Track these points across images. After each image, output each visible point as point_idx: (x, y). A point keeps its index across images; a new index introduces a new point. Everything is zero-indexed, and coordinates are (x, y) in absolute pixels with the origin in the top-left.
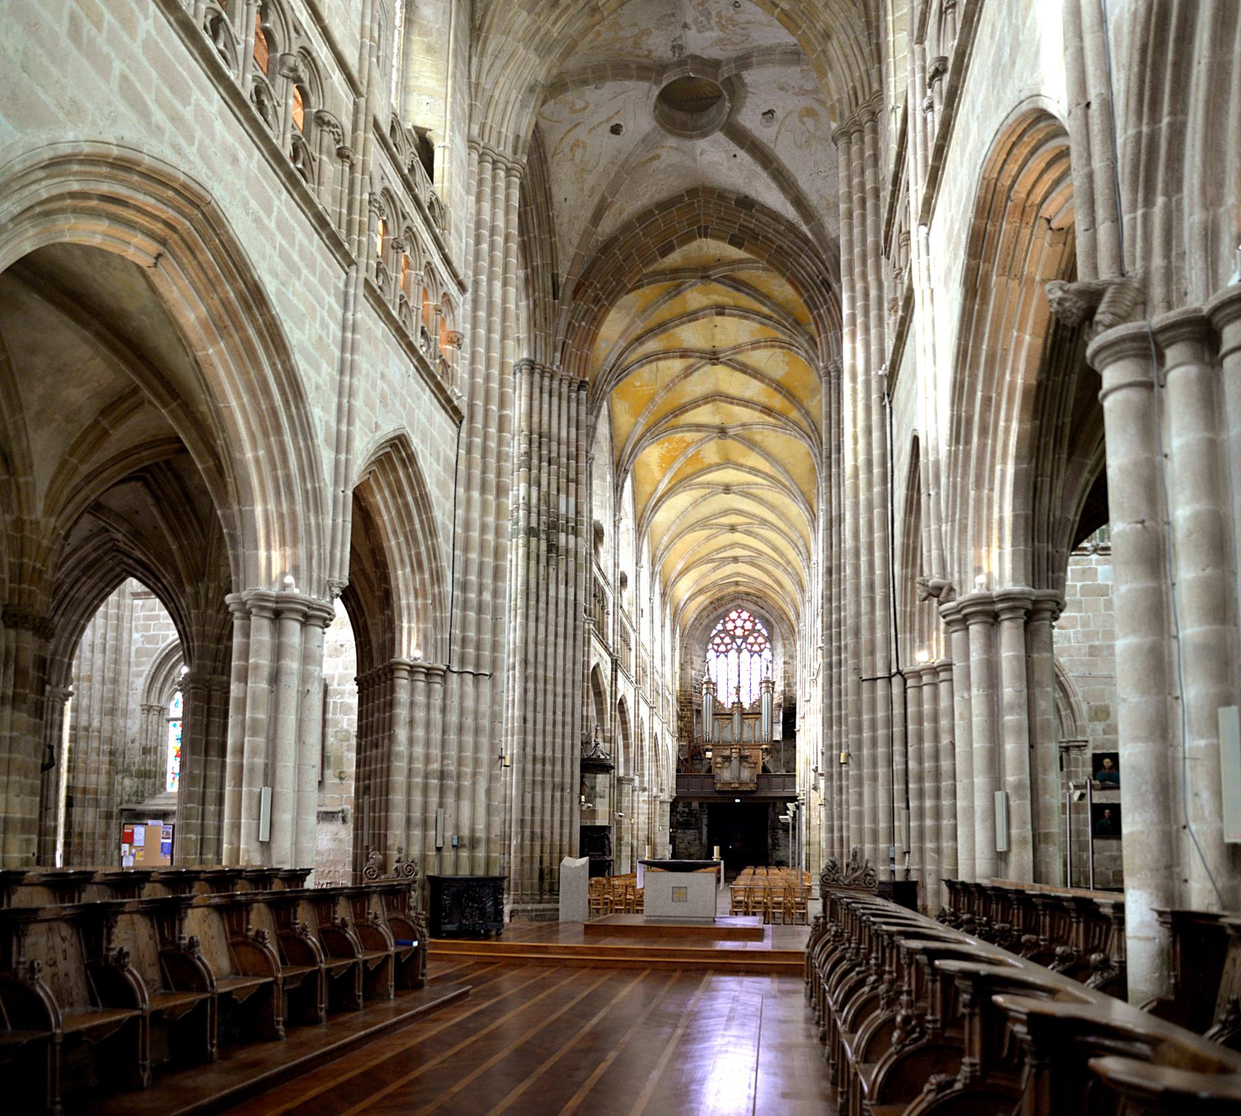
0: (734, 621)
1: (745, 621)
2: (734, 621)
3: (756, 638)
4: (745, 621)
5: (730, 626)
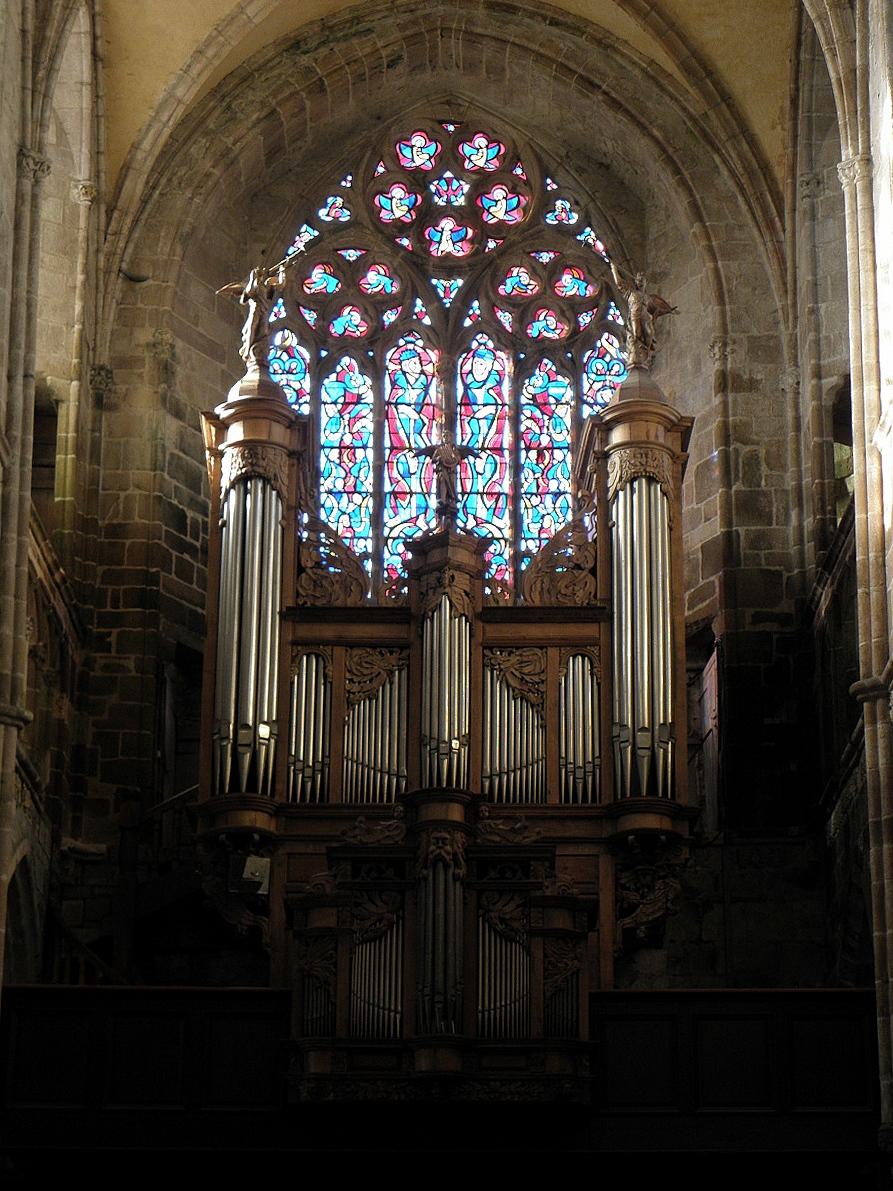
0: (417, 181)
1: (482, 182)
2: (417, 181)
3: (549, 276)
4: (482, 182)
5: (397, 205)
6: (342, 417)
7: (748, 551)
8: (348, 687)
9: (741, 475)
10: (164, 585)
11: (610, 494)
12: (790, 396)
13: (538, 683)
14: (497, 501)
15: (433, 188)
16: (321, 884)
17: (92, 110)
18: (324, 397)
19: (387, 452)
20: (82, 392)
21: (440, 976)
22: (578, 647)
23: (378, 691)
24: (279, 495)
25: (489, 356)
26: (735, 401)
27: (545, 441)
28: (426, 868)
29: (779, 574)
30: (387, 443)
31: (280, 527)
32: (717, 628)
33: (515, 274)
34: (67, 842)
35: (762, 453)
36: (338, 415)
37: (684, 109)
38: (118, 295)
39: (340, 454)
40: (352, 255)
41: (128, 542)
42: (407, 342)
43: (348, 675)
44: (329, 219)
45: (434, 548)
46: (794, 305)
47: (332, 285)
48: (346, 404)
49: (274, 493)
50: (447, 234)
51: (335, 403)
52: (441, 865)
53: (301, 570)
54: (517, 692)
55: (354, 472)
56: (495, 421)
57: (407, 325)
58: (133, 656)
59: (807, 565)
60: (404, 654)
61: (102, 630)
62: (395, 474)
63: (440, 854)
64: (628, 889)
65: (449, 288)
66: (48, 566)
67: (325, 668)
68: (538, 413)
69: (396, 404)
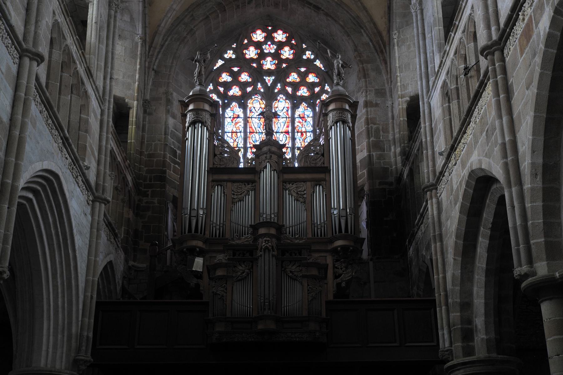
1: (281, 45)
2: (258, 45)
3: (303, 76)
4: (281, 45)
5: (251, 53)
6: (232, 122)
7: (377, 161)
8: (233, 196)
9: (373, 135)
10: (168, 175)
11: (329, 127)
12: (390, 109)
13: (304, 195)
14: (287, 150)
15: (264, 47)
16: (221, 259)
17: (143, 10)
18: (226, 116)
19: (248, 133)
20: (139, 108)
21: (267, 292)
22: (318, 182)
23: (244, 198)
24: (207, 129)
25: (284, 101)
26: (371, 111)
27: (304, 130)
28: (261, 252)
29: (388, 168)
30: (248, 131)
31: (207, 141)
32: (366, 188)
33: (292, 75)
34: (131, 263)
35: (381, 128)
36: (231, 122)
37: (351, 15)
38: (153, 77)
39: (232, 134)
40: (236, 69)
41: (155, 159)
42: (255, 97)
43: (233, 192)
44: (228, 57)
45: (265, 146)
46: (391, 77)
47: (229, 79)
48: (234, 118)
49: (205, 128)
50: (269, 62)
51: (230, 118)
52: (267, 250)
53: (215, 155)
54: (295, 197)
55: (237, 140)
56: (286, 123)
57: (255, 92)
58: (156, 199)
59: (398, 164)
60: (253, 185)
61: (145, 190)
62: (251, 141)
63: (266, 246)
64: (338, 268)
65: (269, 80)
66: (123, 158)
67: (224, 190)
68: (301, 120)
69: (251, 118)
